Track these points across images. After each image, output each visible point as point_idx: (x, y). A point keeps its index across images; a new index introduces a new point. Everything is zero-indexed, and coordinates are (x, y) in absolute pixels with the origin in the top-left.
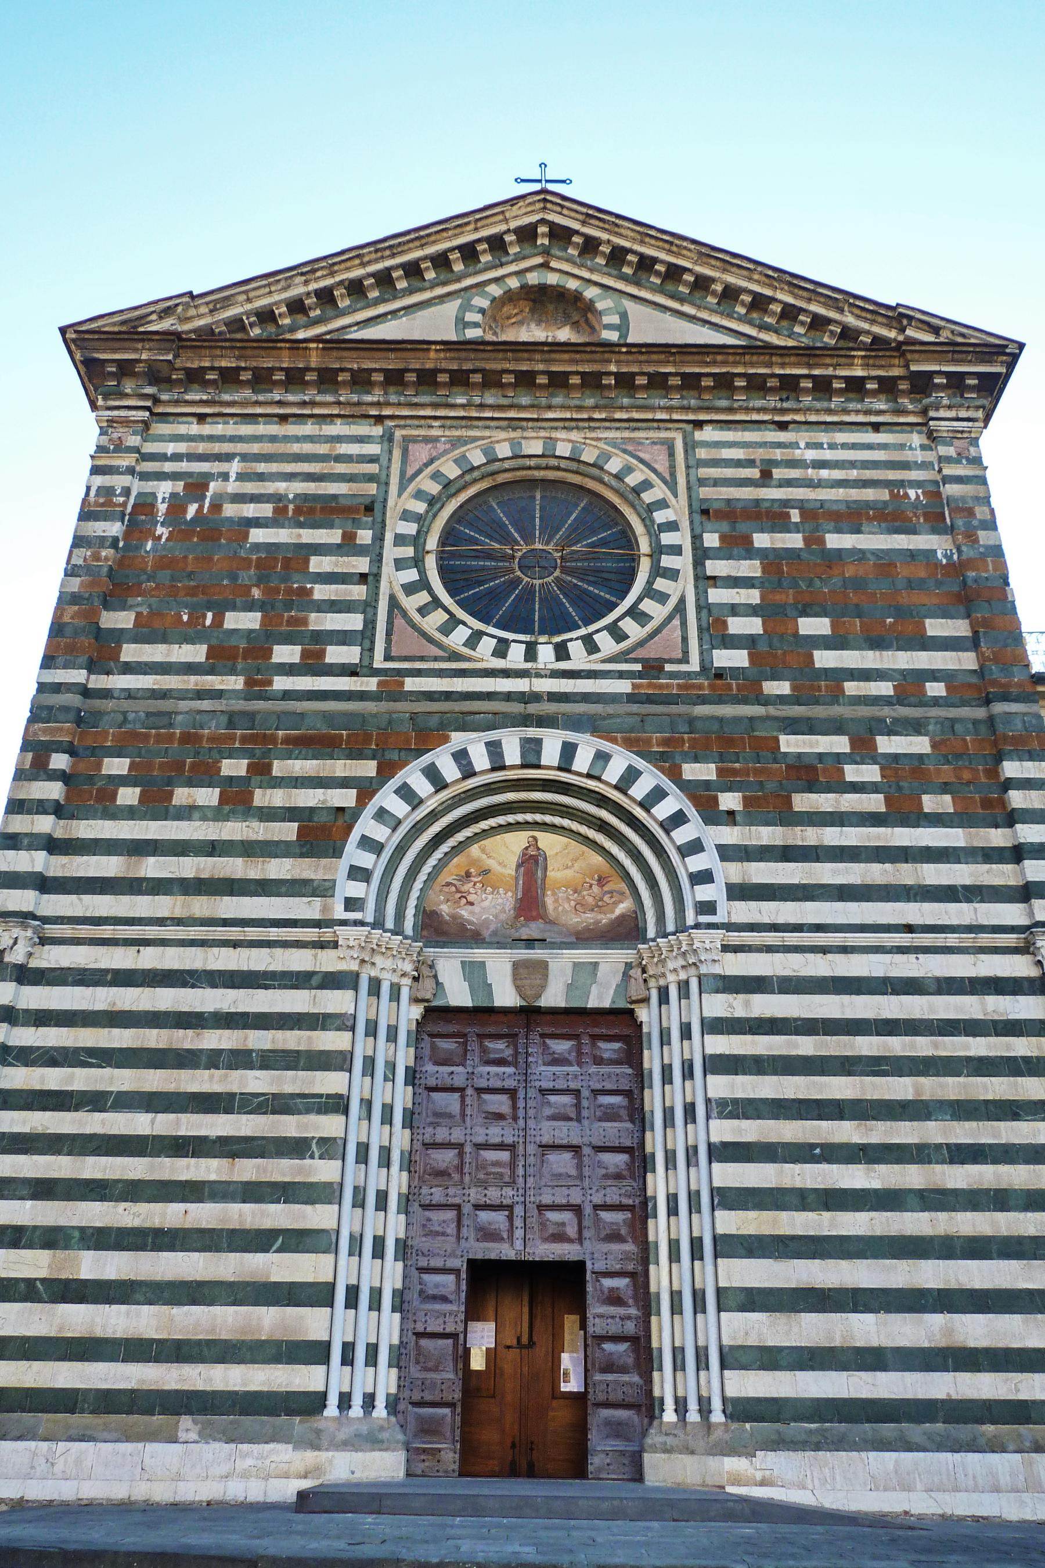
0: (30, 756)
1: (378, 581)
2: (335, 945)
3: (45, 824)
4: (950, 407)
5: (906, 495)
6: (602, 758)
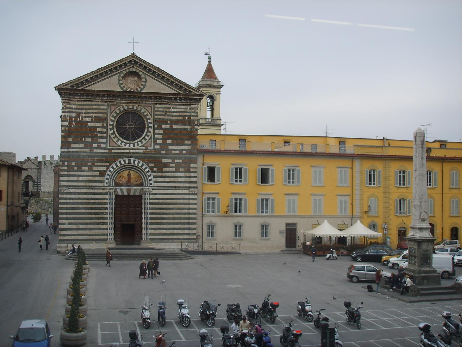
0: (62, 163)
1: (107, 133)
2: (105, 189)
3: (66, 173)
4: (195, 103)
5: (186, 118)
6: (139, 162)
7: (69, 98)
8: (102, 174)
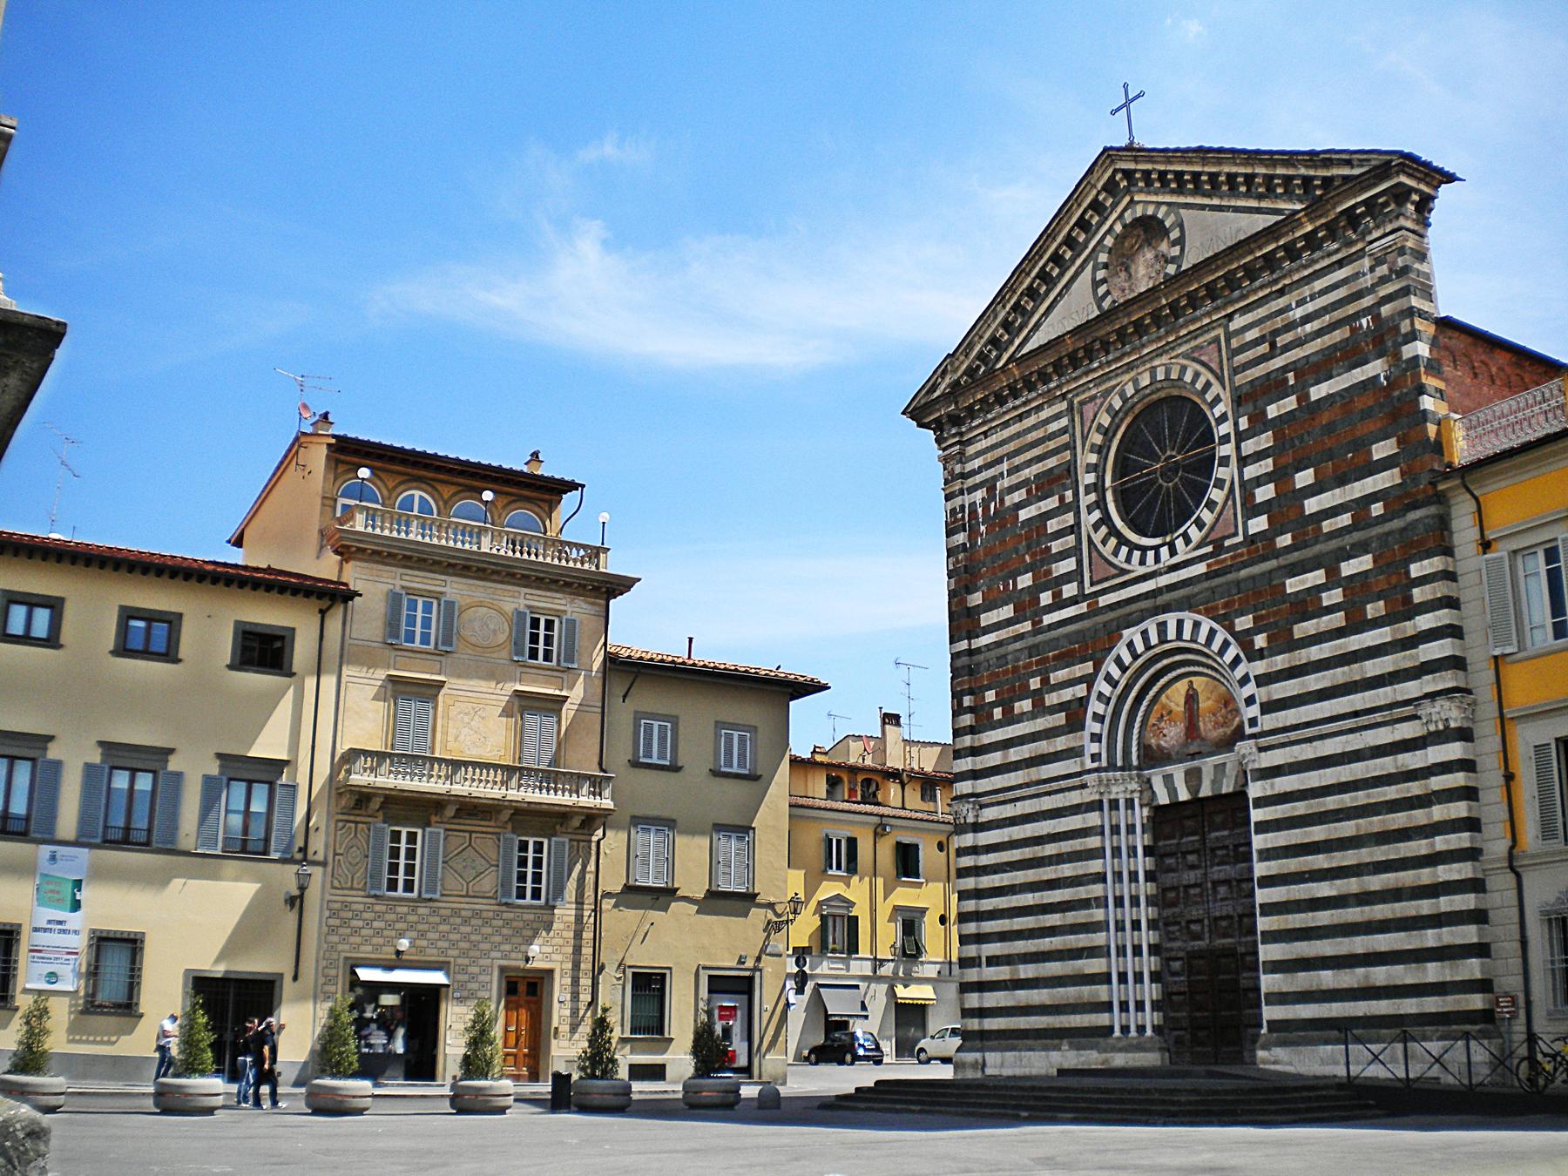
1: (1080, 528)
5: (1361, 325)
6: (1197, 625)
7: (954, 436)
8: (1075, 714)
